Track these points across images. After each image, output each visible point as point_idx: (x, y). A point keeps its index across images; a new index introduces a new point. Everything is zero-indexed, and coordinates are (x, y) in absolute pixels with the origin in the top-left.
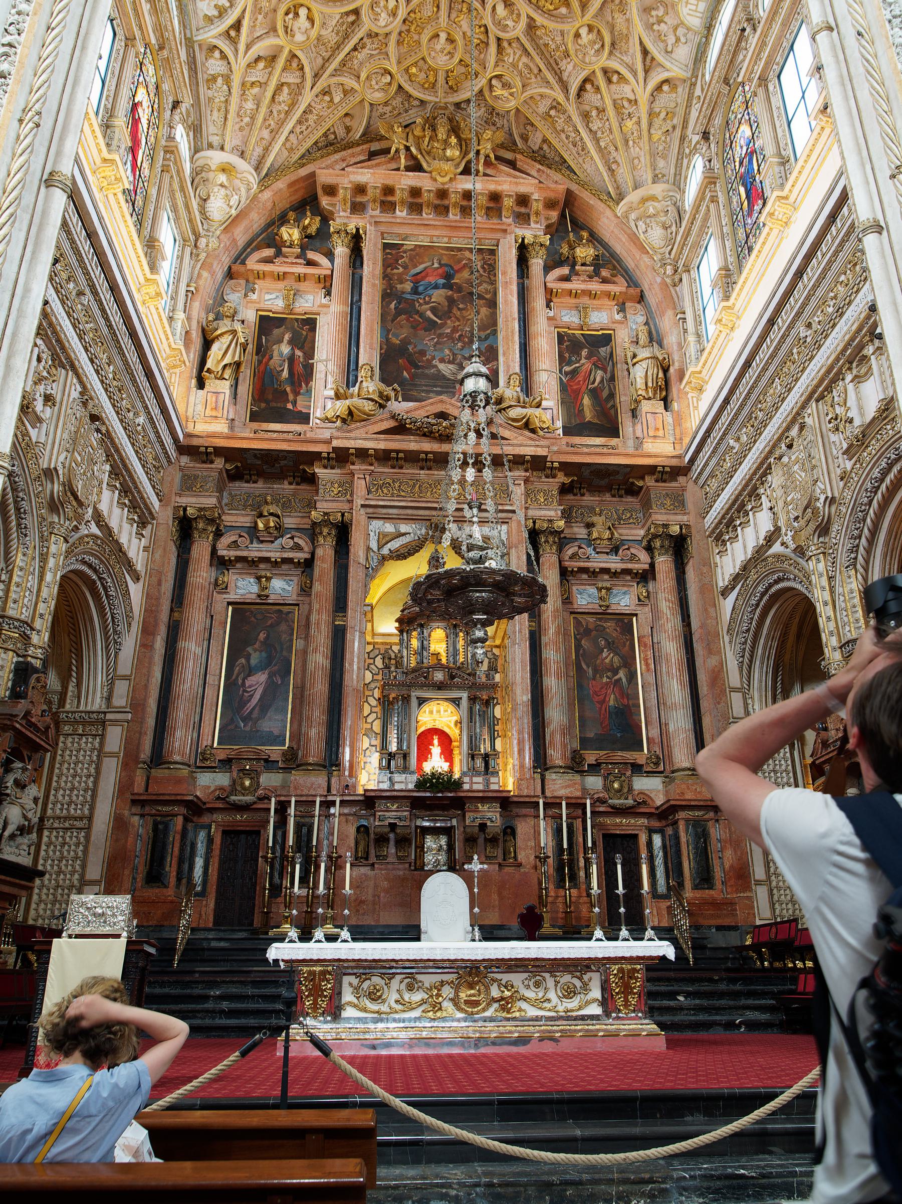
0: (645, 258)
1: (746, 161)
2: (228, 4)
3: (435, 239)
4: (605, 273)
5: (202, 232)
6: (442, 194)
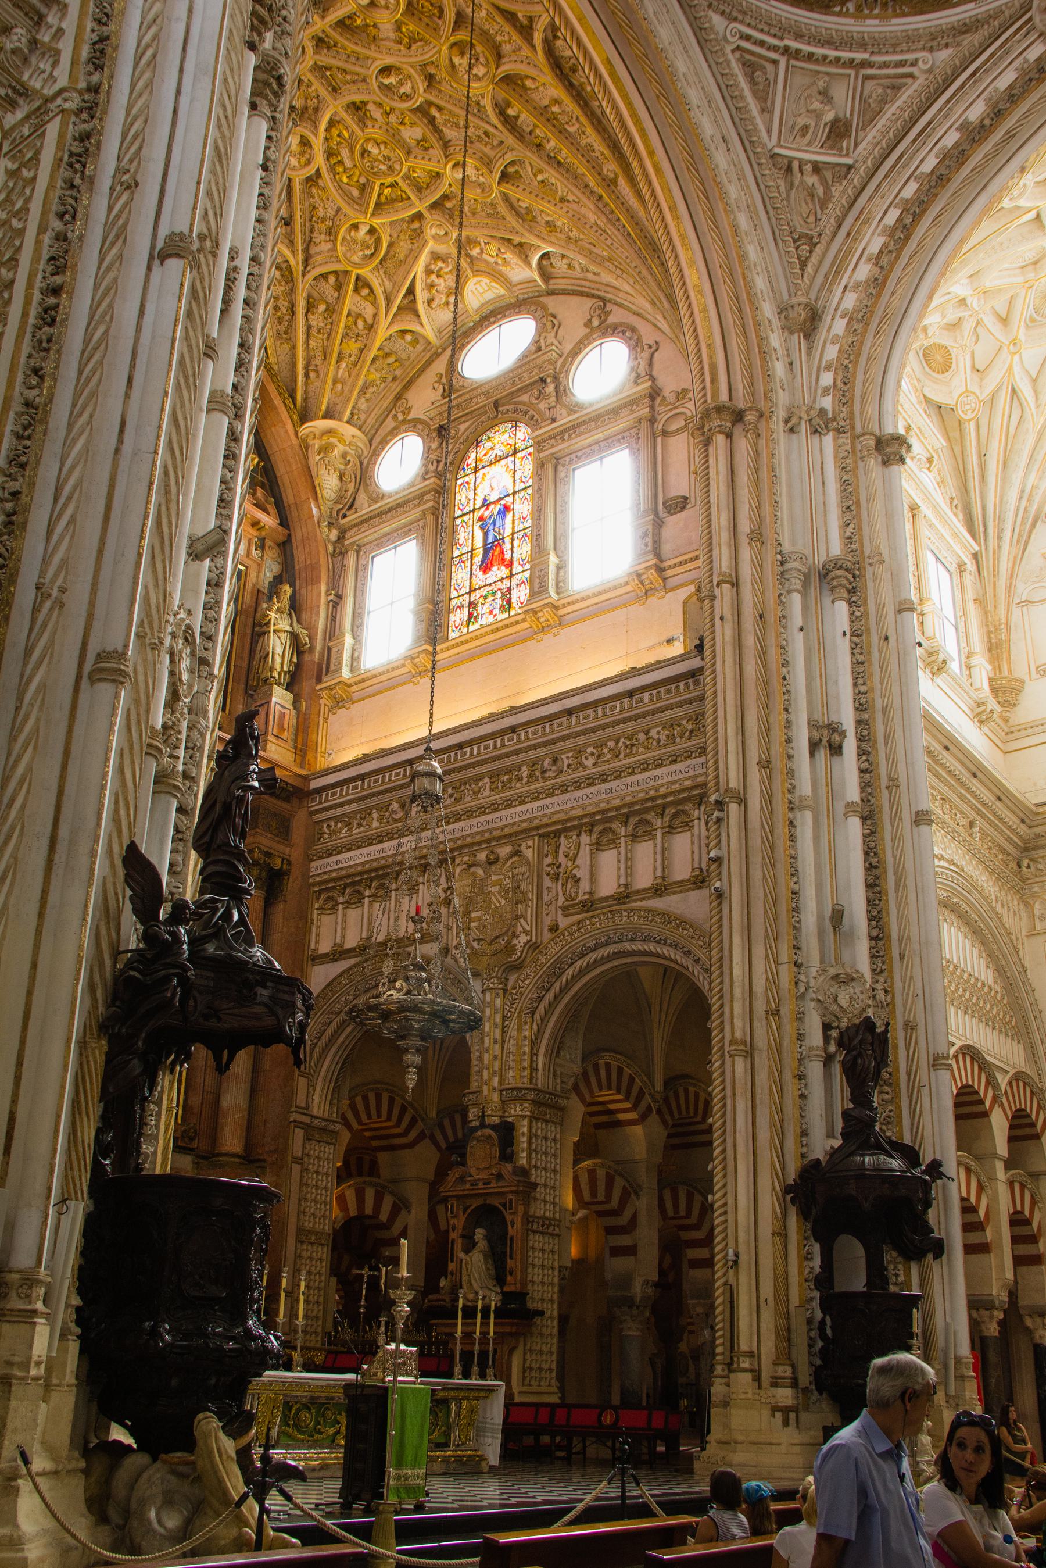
1: (495, 509)
4: (260, 492)
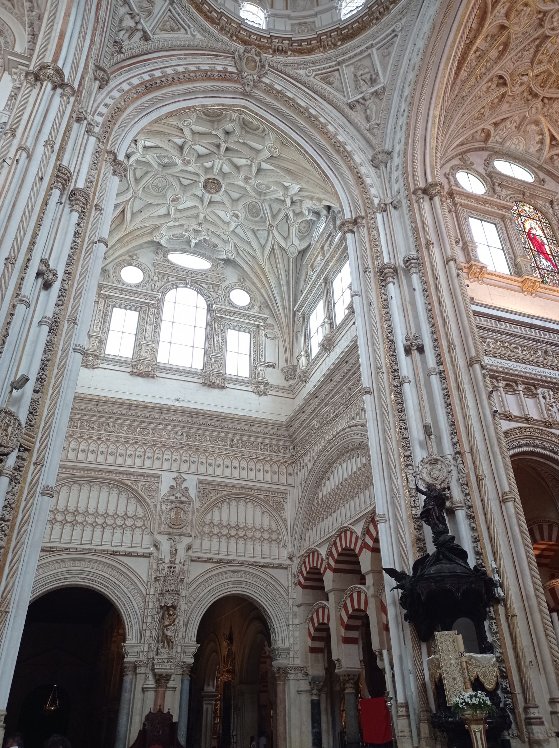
2: (541, 137)
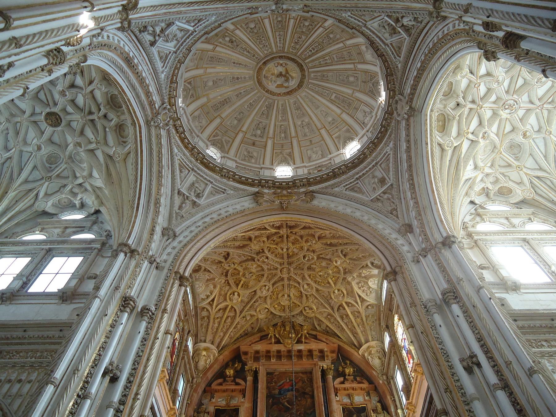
0: (374, 373)
1: (403, 341)
2: (210, 294)
3: (287, 370)
4: (358, 379)
5: (195, 376)
6: (289, 351)
